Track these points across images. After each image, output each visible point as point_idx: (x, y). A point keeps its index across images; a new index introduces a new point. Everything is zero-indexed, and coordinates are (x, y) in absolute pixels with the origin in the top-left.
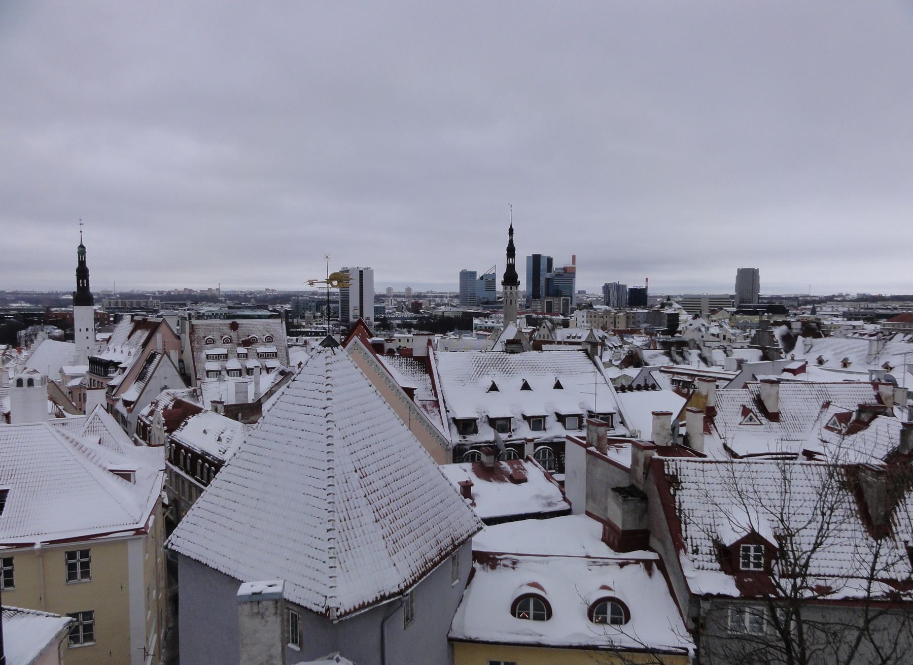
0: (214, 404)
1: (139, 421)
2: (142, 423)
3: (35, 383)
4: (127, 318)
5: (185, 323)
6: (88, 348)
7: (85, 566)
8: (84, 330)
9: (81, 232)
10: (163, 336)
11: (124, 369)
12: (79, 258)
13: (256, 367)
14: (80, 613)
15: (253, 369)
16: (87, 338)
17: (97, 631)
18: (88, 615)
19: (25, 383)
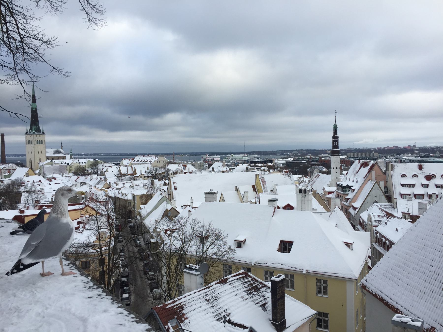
0: (404, 214)
1: (360, 219)
2: (361, 220)
3: (307, 192)
4: (357, 162)
5: (389, 165)
6: (337, 178)
7: (326, 288)
8: (335, 168)
9: (335, 117)
10: (375, 172)
11: (354, 190)
12: (334, 130)
13: (433, 193)
14: (323, 312)
15: (431, 195)
16: (337, 172)
17: (330, 324)
18: (326, 315)
19: (303, 192)
